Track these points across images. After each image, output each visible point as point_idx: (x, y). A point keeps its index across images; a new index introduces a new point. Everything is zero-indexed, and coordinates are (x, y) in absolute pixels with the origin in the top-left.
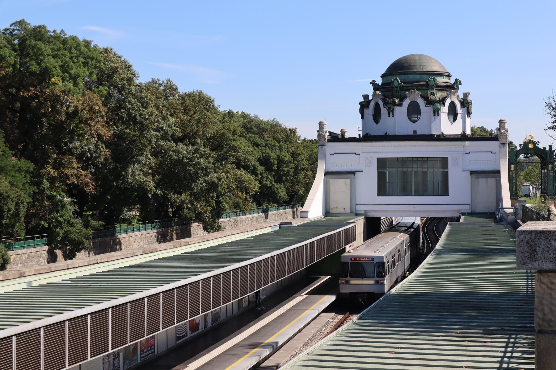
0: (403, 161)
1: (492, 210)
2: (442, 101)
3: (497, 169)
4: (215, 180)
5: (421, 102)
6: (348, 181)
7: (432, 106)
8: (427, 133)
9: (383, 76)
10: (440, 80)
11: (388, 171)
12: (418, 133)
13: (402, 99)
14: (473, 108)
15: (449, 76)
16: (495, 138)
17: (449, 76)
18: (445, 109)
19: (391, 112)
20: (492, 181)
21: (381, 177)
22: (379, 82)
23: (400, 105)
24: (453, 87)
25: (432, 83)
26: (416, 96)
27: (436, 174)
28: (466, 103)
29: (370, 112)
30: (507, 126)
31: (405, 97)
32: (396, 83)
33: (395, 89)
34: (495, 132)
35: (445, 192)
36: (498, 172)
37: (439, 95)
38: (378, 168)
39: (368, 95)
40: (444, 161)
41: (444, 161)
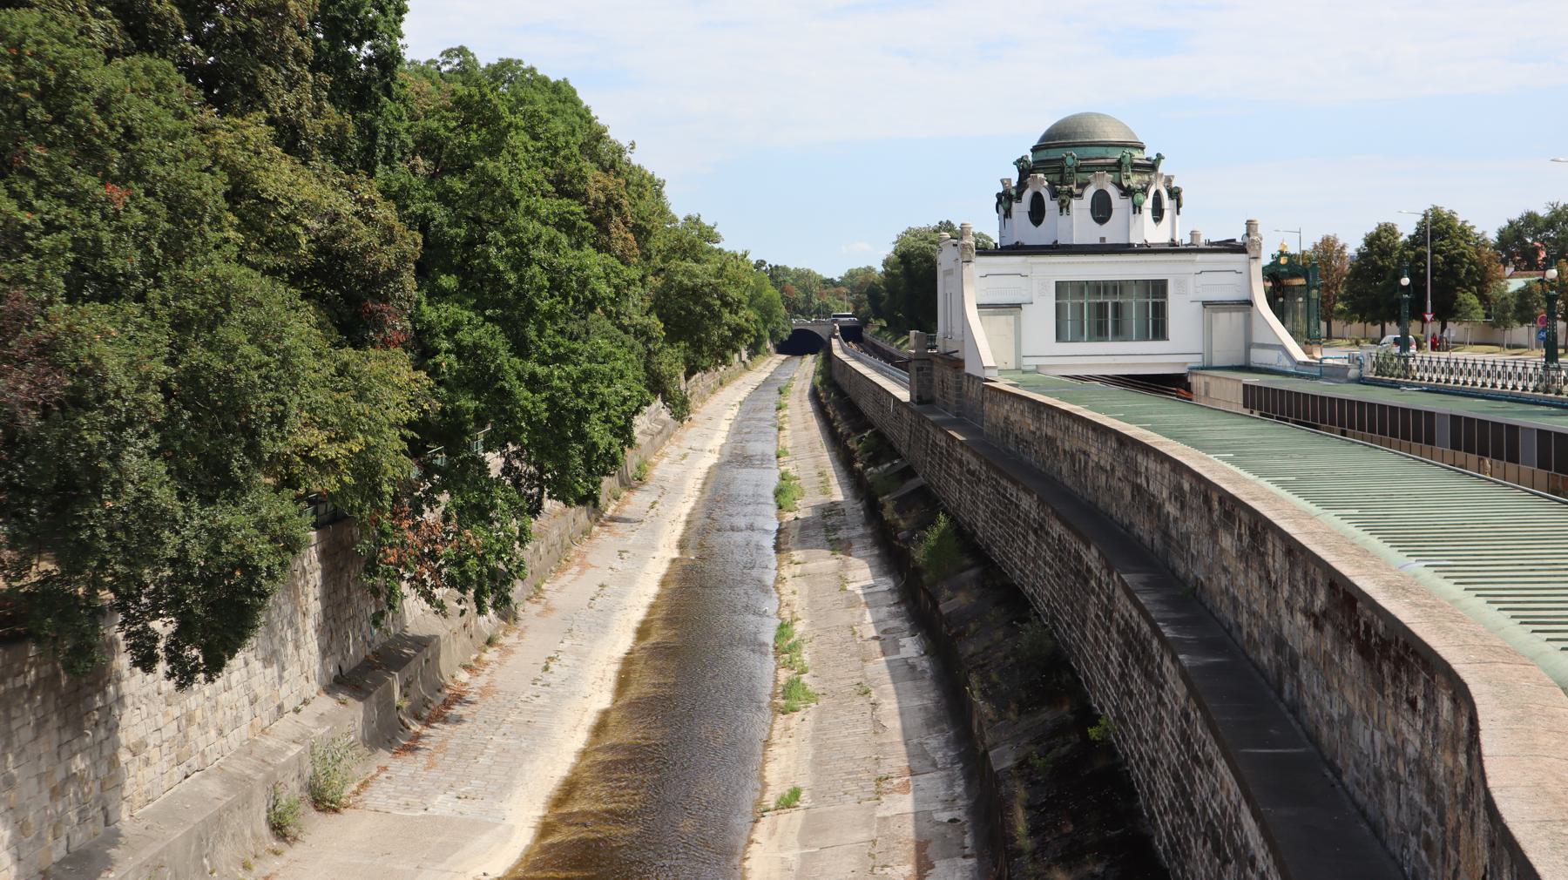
1: (1241, 362)
2: (1145, 191)
3: (1243, 296)
5: (1113, 192)
9: (1035, 150)
10: (1138, 156)
13: (1083, 186)
14: (1184, 201)
16: (1242, 249)
17: (1140, 147)
18: (1148, 204)
19: (1064, 207)
20: (1237, 317)
23: (1080, 196)
24: (1151, 167)
25: (1127, 160)
27: (1134, 305)
28: (1175, 194)
29: (1022, 208)
32: (1069, 161)
33: (1067, 170)
34: (1239, 240)
36: (1249, 303)
37: (1134, 181)
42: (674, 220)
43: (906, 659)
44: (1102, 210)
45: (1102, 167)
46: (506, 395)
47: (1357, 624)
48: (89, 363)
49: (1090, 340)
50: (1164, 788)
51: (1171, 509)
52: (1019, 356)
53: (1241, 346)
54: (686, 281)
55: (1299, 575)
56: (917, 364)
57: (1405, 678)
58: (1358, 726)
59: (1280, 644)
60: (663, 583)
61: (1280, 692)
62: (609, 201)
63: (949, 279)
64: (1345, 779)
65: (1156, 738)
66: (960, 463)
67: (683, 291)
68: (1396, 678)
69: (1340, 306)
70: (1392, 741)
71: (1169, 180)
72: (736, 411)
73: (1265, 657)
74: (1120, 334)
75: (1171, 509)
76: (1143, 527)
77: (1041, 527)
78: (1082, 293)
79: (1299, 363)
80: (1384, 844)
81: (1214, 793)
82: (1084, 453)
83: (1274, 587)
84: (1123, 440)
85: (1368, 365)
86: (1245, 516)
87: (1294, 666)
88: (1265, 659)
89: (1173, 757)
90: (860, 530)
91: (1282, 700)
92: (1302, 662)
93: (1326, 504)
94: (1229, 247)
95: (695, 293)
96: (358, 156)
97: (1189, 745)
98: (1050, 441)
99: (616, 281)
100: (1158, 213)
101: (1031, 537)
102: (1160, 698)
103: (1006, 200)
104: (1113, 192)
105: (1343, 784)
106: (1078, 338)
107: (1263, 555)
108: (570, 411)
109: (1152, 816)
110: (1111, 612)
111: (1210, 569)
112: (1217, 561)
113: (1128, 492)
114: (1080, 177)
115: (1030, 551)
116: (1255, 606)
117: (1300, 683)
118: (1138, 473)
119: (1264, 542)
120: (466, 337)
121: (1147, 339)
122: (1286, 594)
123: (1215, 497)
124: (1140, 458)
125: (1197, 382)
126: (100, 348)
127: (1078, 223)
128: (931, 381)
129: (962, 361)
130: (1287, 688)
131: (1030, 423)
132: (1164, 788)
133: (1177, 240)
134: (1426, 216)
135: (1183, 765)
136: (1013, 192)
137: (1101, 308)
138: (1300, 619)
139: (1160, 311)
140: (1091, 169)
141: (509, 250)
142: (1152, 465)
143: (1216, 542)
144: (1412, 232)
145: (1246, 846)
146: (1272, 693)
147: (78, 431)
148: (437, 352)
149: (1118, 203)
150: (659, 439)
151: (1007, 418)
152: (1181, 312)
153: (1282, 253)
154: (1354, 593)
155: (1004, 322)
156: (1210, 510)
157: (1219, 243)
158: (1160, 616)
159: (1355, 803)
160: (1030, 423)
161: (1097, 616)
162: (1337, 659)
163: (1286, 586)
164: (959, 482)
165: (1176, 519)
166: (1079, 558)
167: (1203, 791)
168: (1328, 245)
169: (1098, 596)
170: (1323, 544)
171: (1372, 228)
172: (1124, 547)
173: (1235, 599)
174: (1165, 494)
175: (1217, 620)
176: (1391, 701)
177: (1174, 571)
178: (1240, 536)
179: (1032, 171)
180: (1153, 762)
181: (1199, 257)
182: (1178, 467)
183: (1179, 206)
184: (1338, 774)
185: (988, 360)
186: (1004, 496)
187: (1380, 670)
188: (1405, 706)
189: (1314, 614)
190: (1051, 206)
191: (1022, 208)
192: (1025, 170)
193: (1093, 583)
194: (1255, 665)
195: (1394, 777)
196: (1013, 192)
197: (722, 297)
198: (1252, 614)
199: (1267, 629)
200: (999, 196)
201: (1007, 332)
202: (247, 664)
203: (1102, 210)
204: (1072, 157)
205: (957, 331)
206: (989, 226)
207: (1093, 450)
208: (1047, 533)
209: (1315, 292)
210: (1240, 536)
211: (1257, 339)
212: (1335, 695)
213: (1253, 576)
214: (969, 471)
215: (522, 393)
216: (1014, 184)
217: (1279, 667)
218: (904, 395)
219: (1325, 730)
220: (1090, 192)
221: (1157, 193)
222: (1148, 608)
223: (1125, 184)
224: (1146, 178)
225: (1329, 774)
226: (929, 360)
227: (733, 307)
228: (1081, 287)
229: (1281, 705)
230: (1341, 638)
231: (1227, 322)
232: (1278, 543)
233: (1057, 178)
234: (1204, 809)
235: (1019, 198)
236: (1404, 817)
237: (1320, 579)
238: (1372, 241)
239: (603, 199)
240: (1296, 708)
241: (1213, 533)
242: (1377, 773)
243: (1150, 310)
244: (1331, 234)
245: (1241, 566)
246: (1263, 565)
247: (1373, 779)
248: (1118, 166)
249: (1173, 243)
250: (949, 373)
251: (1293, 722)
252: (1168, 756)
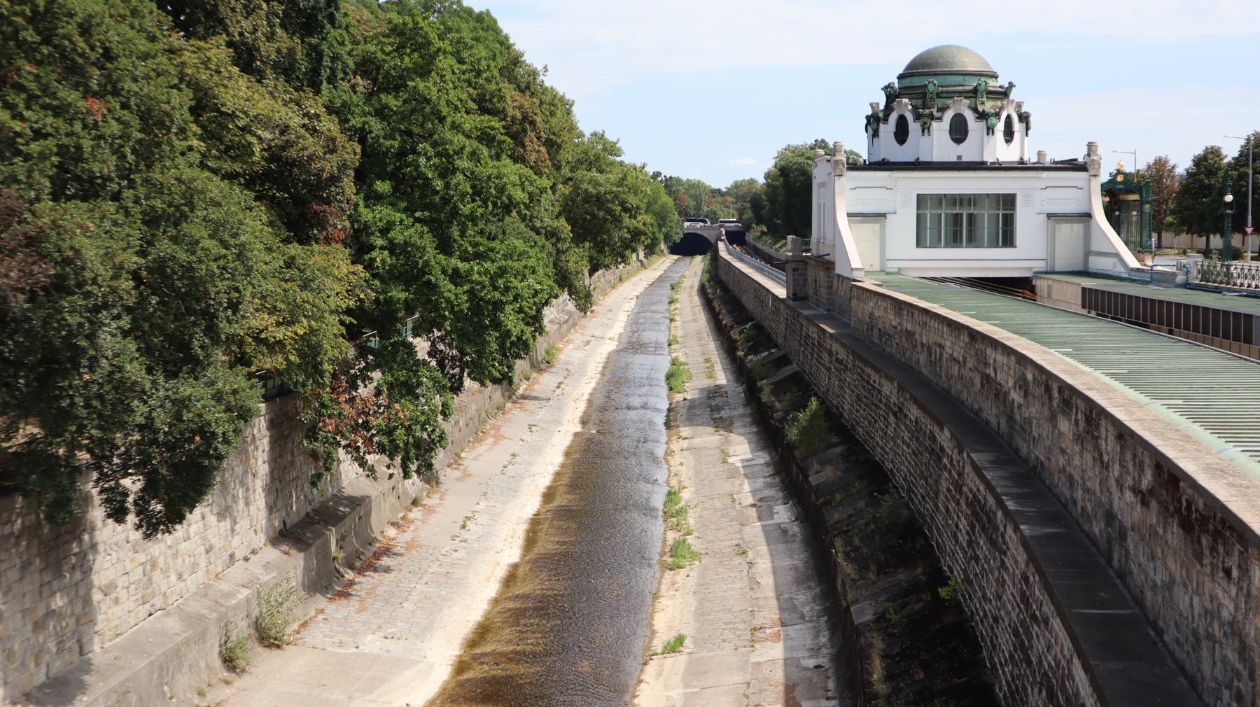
1: (1080, 268)
2: (998, 115)
4: (640, 226)
5: (969, 116)
6: (877, 226)
8: (977, 159)
9: (901, 77)
10: (993, 84)
11: (928, 213)
12: (964, 159)
13: (943, 110)
16: (1082, 168)
17: (994, 76)
18: (1000, 127)
19: (926, 129)
20: (1078, 228)
22: (896, 85)
23: (940, 119)
24: (1004, 94)
25: (982, 88)
26: (963, 107)
27: (986, 216)
28: (1024, 118)
29: (888, 129)
30: (1100, 151)
31: (947, 108)
32: (931, 88)
33: (929, 96)
34: (1081, 160)
35: (1008, 240)
36: (1088, 216)
38: (918, 209)
39: (878, 104)
40: (1008, 201)
41: (1008, 201)
42: (581, 135)
43: (779, 525)
44: (959, 132)
45: (960, 93)
46: (433, 287)
47: (1180, 501)
48: (70, 253)
49: (947, 246)
50: (1006, 642)
51: (1016, 396)
52: (883, 259)
53: (1080, 253)
54: (591, 189)
55: (1129, 456)
56: (794, 265)
57: (1221, 549)
58: (1179, 591)
59: (1110, 517)
60: (567, 454)
61: (1109, 559)
62: (525, 118)
63: (822, 190)
64: (1166, 638)
65: (999, 597)
66: (830, 353)
67: (588, 198)
68: (1213, 550)
69: (1170, 219)
70: (1209, 606)
71: (1019, 105)
72: (633, 304)
73: (1097, 528)
74: (973, 241)
75: (1016, 396)
76: (991, 412)
77: (900, 410)
78: (940, 205)
79: (1132, 269)
80: (1200, 697)
81: (1049, 647)
82: (940, 346)
83: (1106, 467)
84: (974, 335)
85: (1194, 272)
86: (1080, 403)
87: (1123, 537)
88: (1096, 530)
89: (1014, 615)
90: (741, 410)
91: (1112, 567)
92: (1130, 533)
93: (1154, 394)
94: (1072, 166)
95: (599, 200)
96: (305, 76)
97: (1027, 604)
98: (910, 335)
99: (530, 189)
100: (1009, 134)
101: (892, 419)
102: (1003, 562)
103: (874, 122)
104: (969, 116)
105: (1164, 642)
106: (936, 244)
107: (1096, 438)
108: (488, 302)
109: (994, 667)
110: (961, 487)
111: (1049, 450)
112: (1056, 448)
113: (977, 381)
114: (940, 102)
115: (890, 432)
116: (1089, 484)
117: (1127, 552)
118: (986, 365)
119: (1098, 427)
120: (398, 235)
121: (997, 246)
122: (1117, 474)
123: (1055, 387)
124: (989, 351)
125: (1041, 285)
126: (81, 241)
127: (936, 142)
128: (805, 280)
129: (833, 263)
130: (1116, 556)
131: (892, 319)
132: (1006, 642)
133: (1026, 159)
134: (1248, 140)
135: (1022, 622)
136: (881, 115)
137: (957, 219)
138: (1129, 495)
140: (951, 94)
141: (436, 160)
142: (1000, 357)
143: (1055, 427)
144: (1236, 154)
145: (1077, 694)
146: (1102, 561)
147: (61, 313)
148: (372, 248)
149: (973, 125)
150: (565, 327)
151: (871, 314)
152: (1027, 223)
153: (1119, 172)
154: (1178, 475)
155: (870, 229)
156: (1050, 398)
157: (1062, 162)
158: (1005, 490)
159: (1175, 660)
160: (892, 319)
161: (949, 490)
162: (1161, 531)
163: (1117, 467)
164: (829, 369)
165: (1020, 406)
166: (933, 439)
167: (1039, 646)
168: (1160, 166)
169: (950, 472)
170: (1150, 430)
171: (1199, 151)
172: (973, 430)
173: (1071, 477)
174: (1010, 384)
175: (1055, 495)
176: (1208, 570)
177: (1017, 451)
178: (1077, 422)
179: (899, 95)
180: (996, 619)
181: (1045, 174)
182: (1022, 359)
183: (1027, 128)
184: (1160, 633)
185: (856, 262)
186: (868, 383)
187: (1199, 543)
188: (1221, 574)
189: (1141, 492)
190: (914, 127)
191: (888, 129)
192: (892, 95)
193: (945, 460)
194: (1088, 536)
195: (1210, 637)
196: (881, 115)
197: (622, 204)
198: (1087, 490)
199: (1099, 504)
200: (868, 118)
201: (874, 239)
202: (203, 518)
203: (959, 132)
204: (933, 84)
205: (829, 236)
206: (858, 143)
207: (948, 343)
208: (906, 416)
209: (1147, 206)
210: (1077, 422)
211: (1095, 247)
212: (1159, 563)
213: (1088, 457)
214: (837, 360)
215: (446, 286)
216: (882, 107)
217: (1109, 538)
218: (781, 292)
219: (1149, 594)
220: (949, 115)
221: (1009, 117)
222: (994, 483)
223: (980, 108)
224: (999, 103)
225: (1152, 633)
226: (804, 261)
227: (632, 212)
228: (939, 199)
229: (1113, 574)
230: (1165, 511)
231: (1069, 233)
232: (1111, 428)
233: (919, 102)
234: (1040, 662)
235: (886, 120)
236: (1218, 673)
237: (1147, 460)
238: (1199, 162)
239: (519, 116)
240: (1123, 574)
241: (1053, 418)
242: (1195, 633)
243: (1002, 221)
244: (1163, 155)
245: (1077, 448)
246: (1097, 447)
247: (1191, 638)
248: (974, 93)
249: (1022, 162)
250: (822, 274)
251: (1121, 587)
252: (1008, 614)
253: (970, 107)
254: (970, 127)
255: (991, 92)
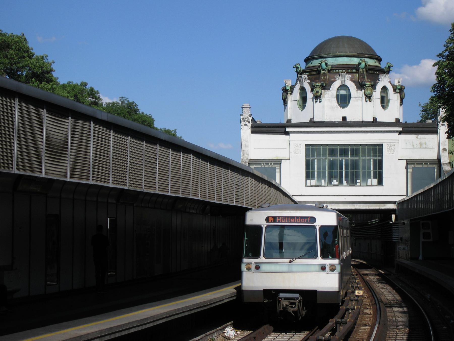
0: (332, 149)
2: (373, 87)
7: (363, 91)
9: (307, 60)
15: (379, 60)
17: (379, 60)
19: (317, 97)
21: (309, 165)
38: (306, 156)
40: (378, 149)
41: (378, 149)
100: (384, 102)
127: (326, 108)
136: (288, 88)
139: (379, 165)
190: (310, 95)
221: (384, 89)
253: (351, 80)
254: (352, 95)
255: (370, 69)
